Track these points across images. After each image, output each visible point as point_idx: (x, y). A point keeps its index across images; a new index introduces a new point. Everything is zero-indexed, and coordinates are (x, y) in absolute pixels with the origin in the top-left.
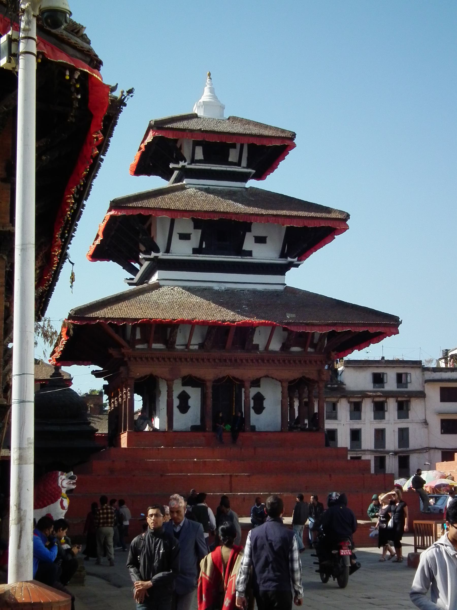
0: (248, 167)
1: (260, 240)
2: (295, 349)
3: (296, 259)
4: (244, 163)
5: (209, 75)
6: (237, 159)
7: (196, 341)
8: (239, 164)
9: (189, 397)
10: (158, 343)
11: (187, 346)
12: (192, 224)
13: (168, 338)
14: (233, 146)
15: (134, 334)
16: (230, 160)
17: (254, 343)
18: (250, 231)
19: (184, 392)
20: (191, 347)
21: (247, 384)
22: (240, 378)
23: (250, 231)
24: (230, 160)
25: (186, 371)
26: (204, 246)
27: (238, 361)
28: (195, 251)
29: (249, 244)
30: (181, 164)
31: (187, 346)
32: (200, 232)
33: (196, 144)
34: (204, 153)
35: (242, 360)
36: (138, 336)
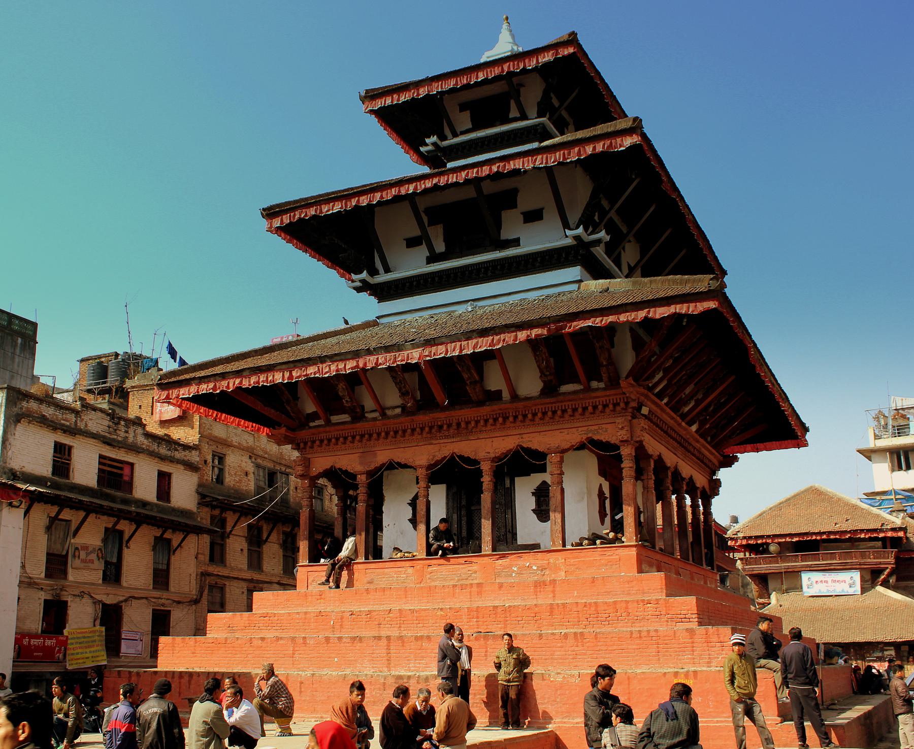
0: (539, 116)
4: (532, 111)
5: (507, 18)
8: (524, 117)
16: (511, 116)
18: (514, 205)
22: (472, 457)
23: (514, 205)
24: (511, 116)
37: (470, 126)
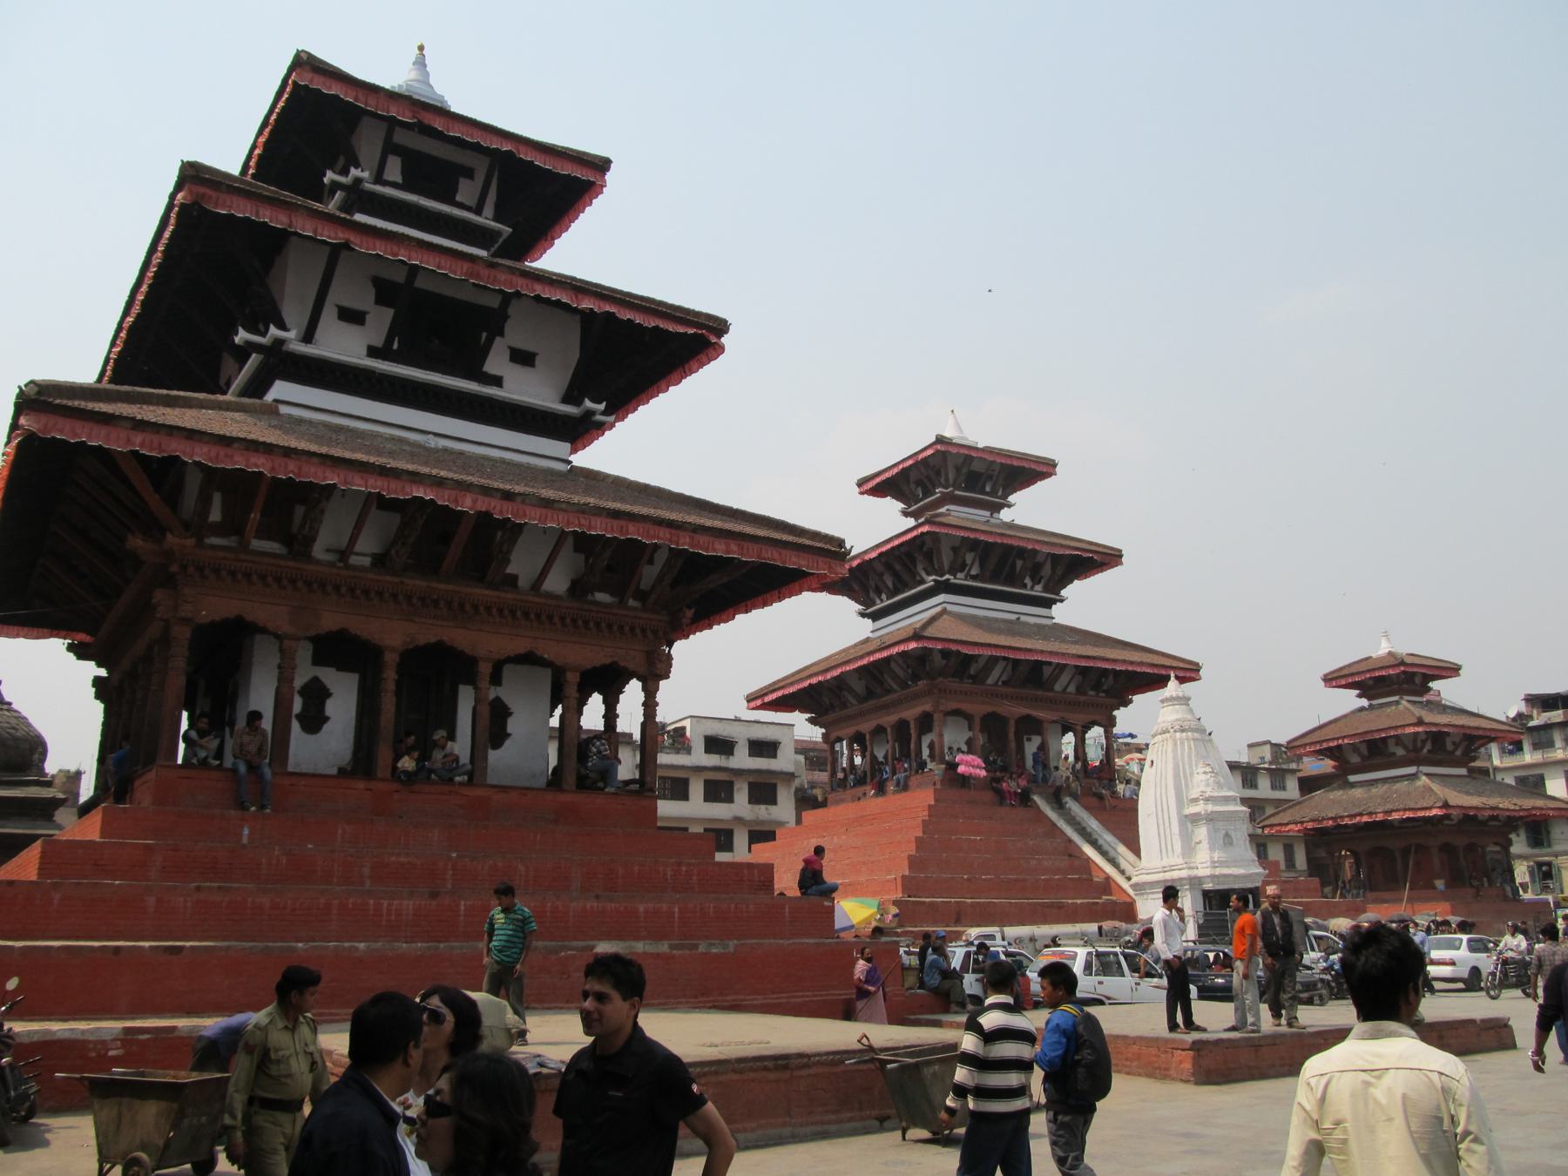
0: (496, 219)
1: (523, 358)
2: (602, 597)
3: (602, 407)
4: (489, 210)
6: (473, 204)
7: (368, 545)
8: (478, 211)
9: (329, 695)
10: (269, 539)
11: (344, 554)
12: (371, 293)
13: (295, 529)
14: (469, 173)
15: (205, 501)
16: (458, 198)
17: (508, 571)
18: (502, 334)
19: (316, 680)
20: (354, 560)
21: (485, 669)
23: (502, 334)
24: (458, 198)
25: (330, 620)
26: (395, 346)
27: (468, 607)
30: (354, 172)
31: (344, 554)
32: (389, 313)
33: (390, 148)
34: (404, 172)
35: (475, 607)
36: (215, 515)
37: (399, 180)
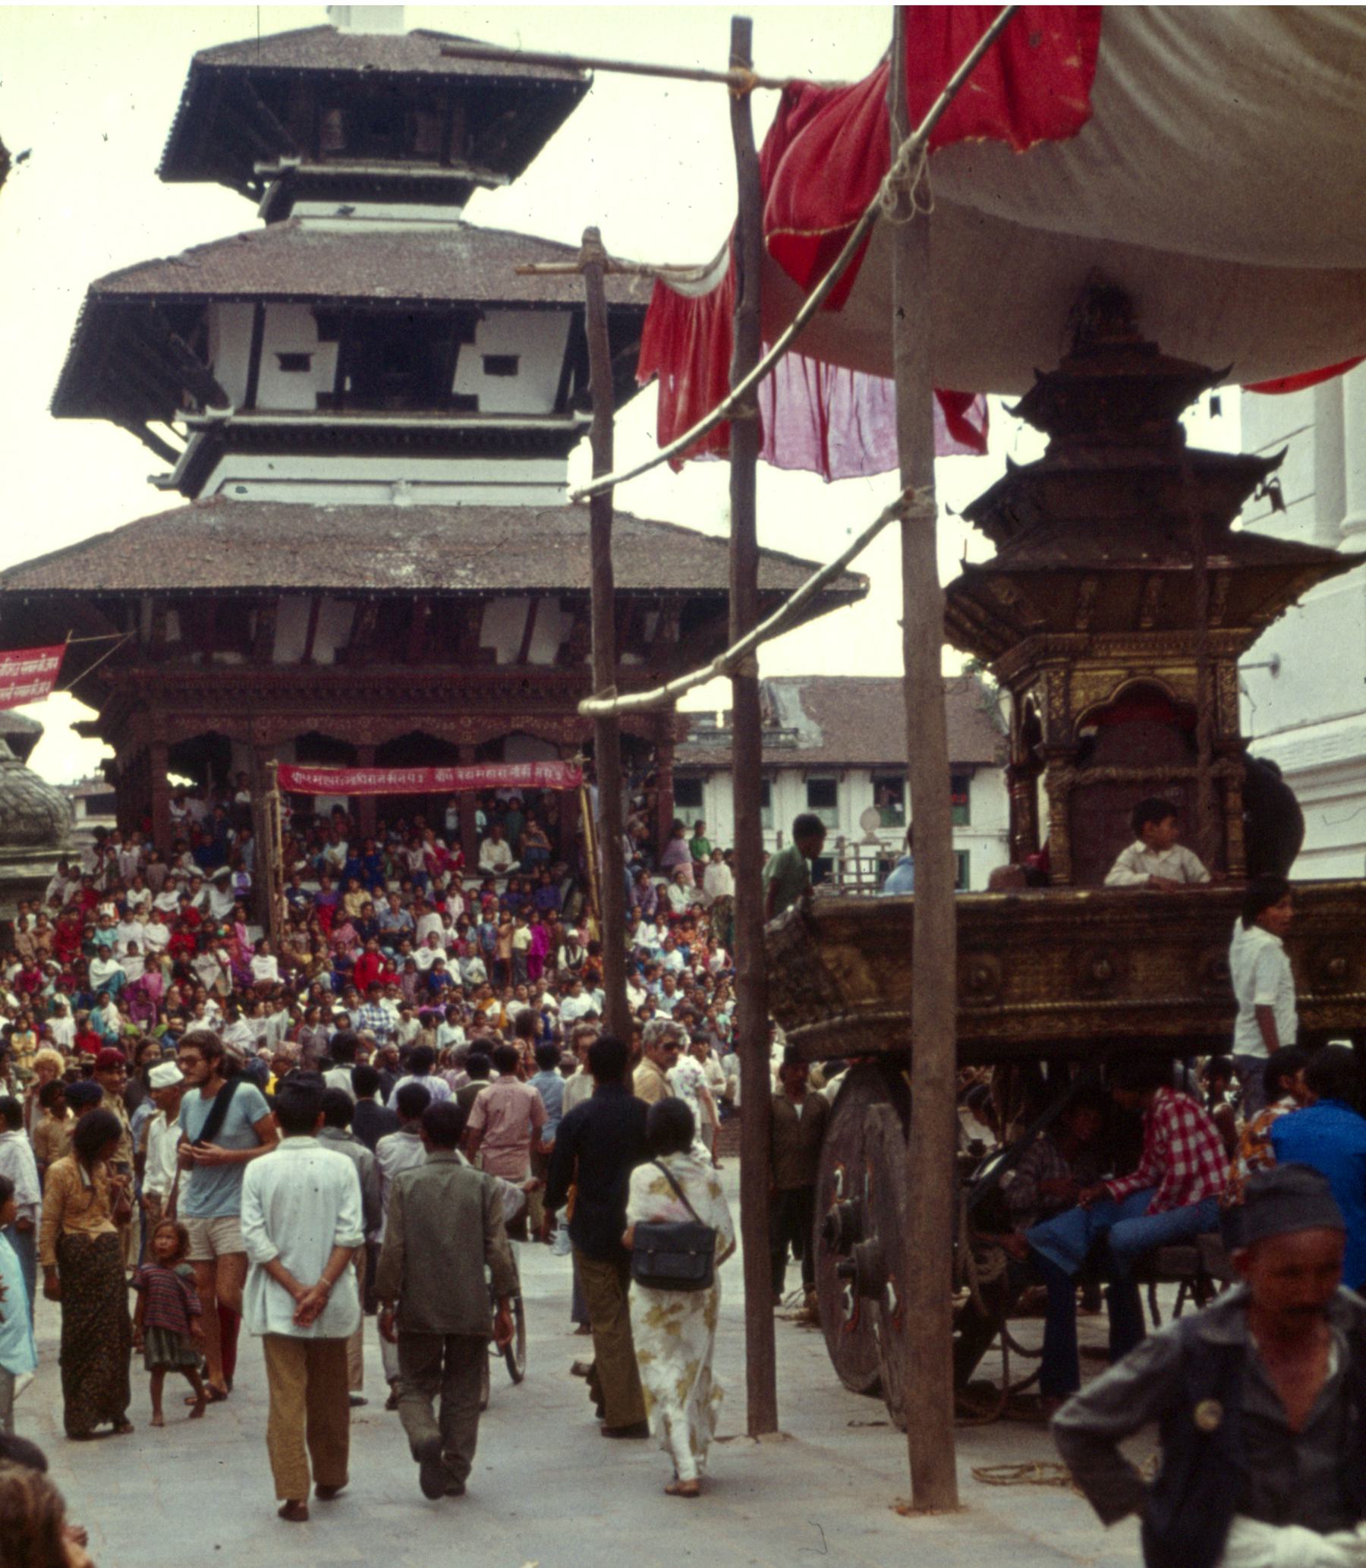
1: (501, 366)
26: (348, 386)
28: (326, 402)
29: (469, 377)
